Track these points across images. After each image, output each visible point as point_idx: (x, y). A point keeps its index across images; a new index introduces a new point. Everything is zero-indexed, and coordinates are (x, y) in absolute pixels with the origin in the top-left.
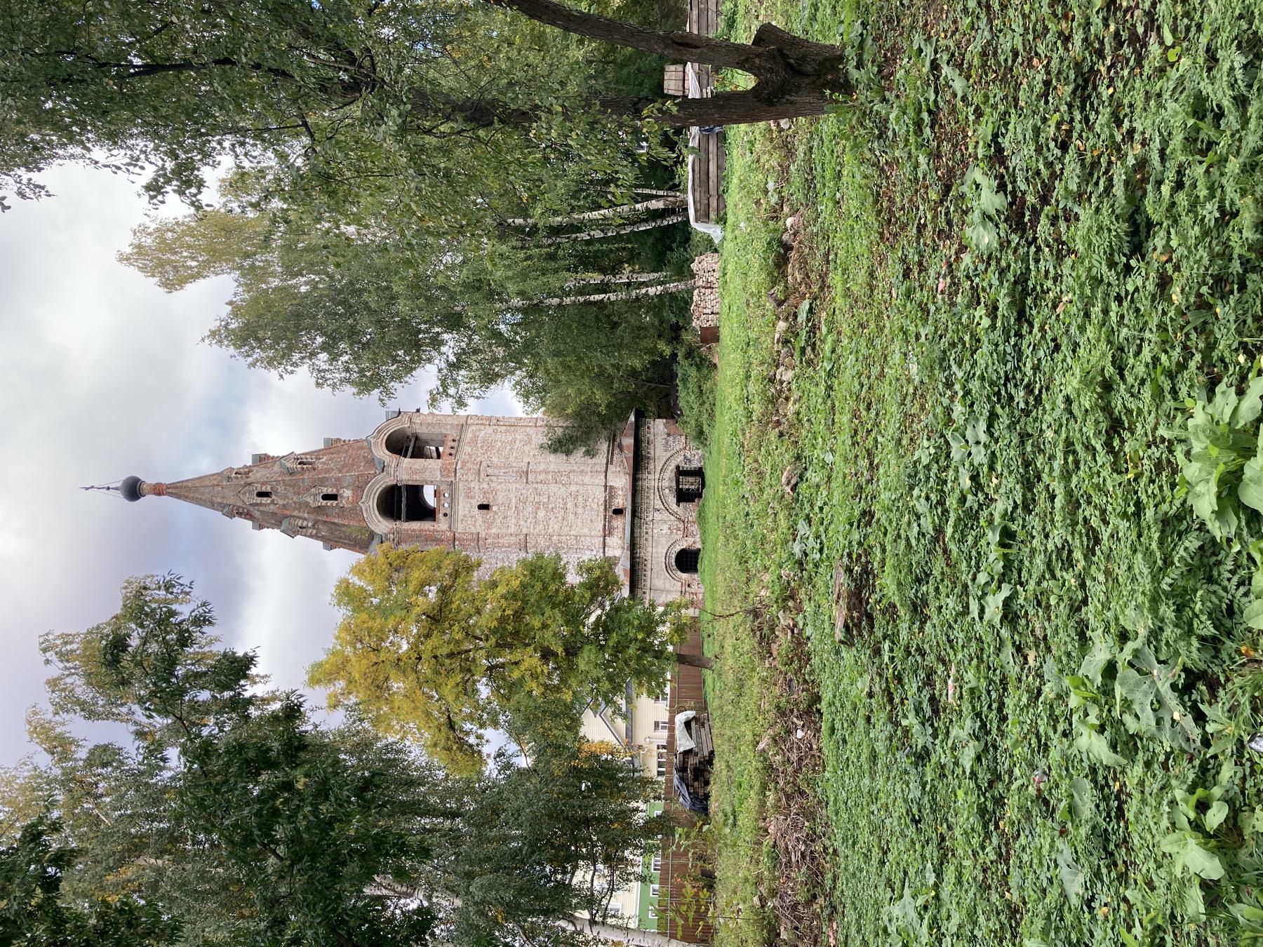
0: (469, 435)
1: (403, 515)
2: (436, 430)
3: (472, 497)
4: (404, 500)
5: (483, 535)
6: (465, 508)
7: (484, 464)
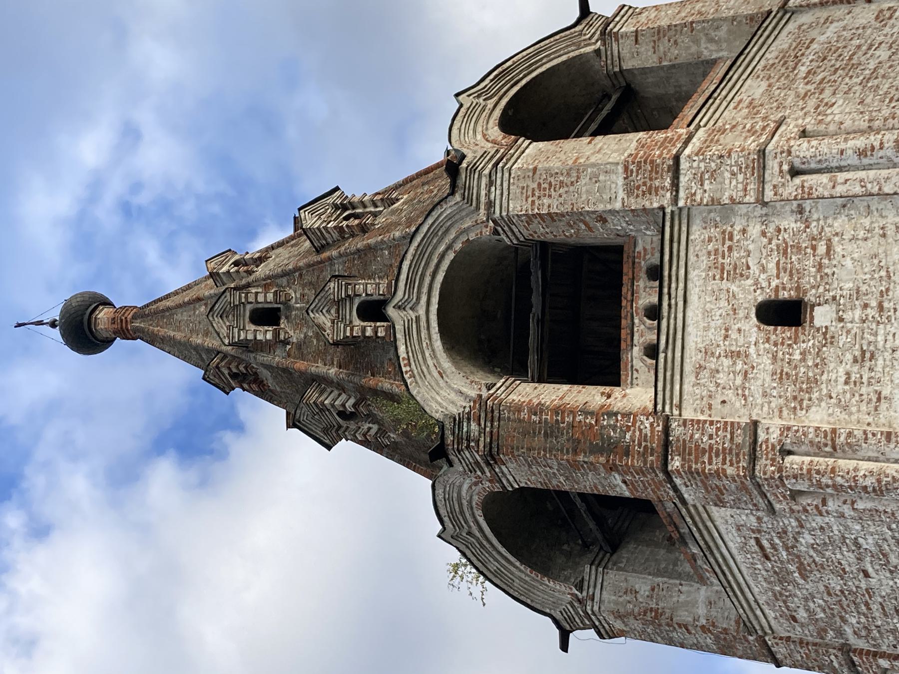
0: (783, 41)
1: (532, 359)
2: (681, 52)
3: (738, 273)
4: (536, 300)
5: (771, 431)
6: (710, 312)
7: (791, 128)
